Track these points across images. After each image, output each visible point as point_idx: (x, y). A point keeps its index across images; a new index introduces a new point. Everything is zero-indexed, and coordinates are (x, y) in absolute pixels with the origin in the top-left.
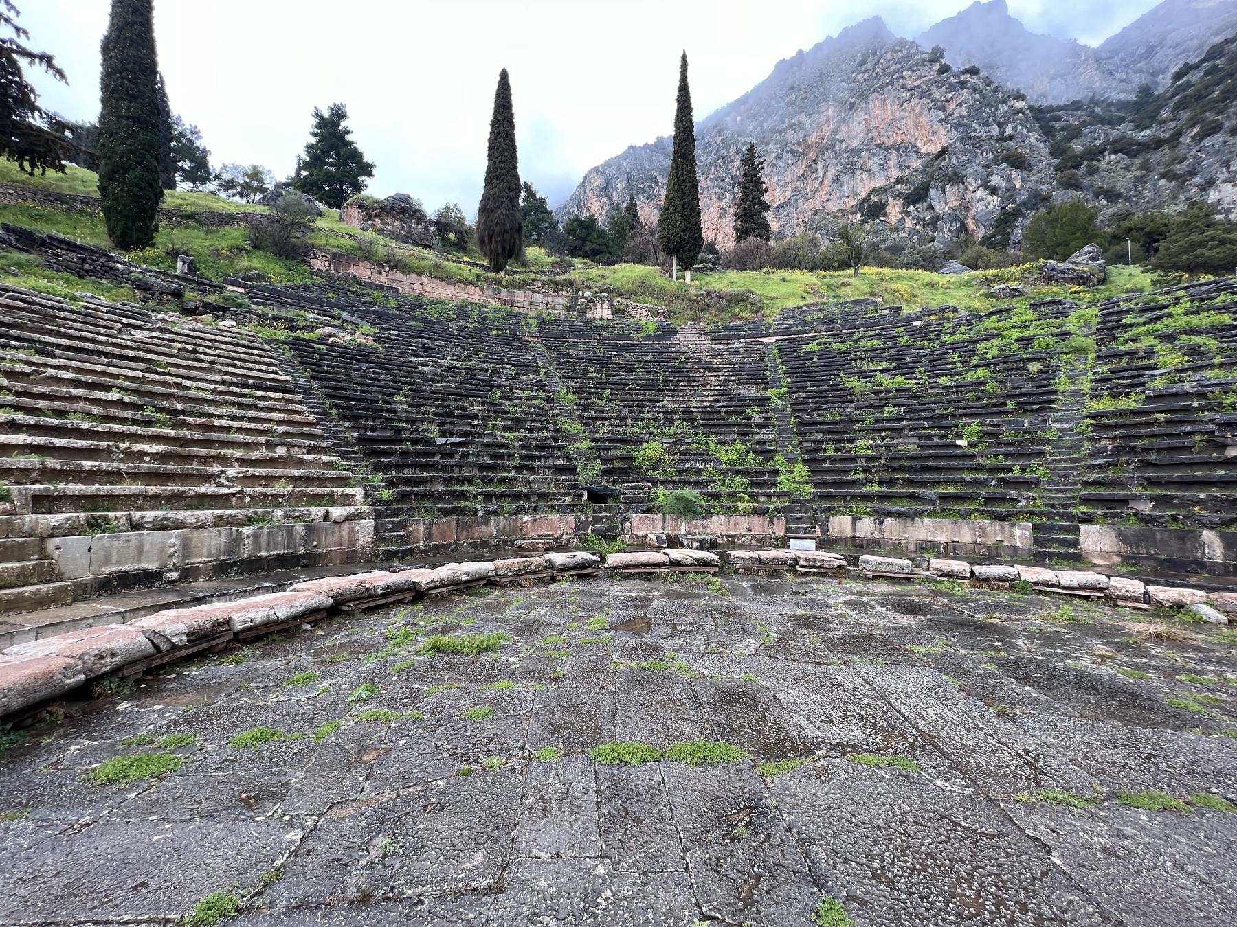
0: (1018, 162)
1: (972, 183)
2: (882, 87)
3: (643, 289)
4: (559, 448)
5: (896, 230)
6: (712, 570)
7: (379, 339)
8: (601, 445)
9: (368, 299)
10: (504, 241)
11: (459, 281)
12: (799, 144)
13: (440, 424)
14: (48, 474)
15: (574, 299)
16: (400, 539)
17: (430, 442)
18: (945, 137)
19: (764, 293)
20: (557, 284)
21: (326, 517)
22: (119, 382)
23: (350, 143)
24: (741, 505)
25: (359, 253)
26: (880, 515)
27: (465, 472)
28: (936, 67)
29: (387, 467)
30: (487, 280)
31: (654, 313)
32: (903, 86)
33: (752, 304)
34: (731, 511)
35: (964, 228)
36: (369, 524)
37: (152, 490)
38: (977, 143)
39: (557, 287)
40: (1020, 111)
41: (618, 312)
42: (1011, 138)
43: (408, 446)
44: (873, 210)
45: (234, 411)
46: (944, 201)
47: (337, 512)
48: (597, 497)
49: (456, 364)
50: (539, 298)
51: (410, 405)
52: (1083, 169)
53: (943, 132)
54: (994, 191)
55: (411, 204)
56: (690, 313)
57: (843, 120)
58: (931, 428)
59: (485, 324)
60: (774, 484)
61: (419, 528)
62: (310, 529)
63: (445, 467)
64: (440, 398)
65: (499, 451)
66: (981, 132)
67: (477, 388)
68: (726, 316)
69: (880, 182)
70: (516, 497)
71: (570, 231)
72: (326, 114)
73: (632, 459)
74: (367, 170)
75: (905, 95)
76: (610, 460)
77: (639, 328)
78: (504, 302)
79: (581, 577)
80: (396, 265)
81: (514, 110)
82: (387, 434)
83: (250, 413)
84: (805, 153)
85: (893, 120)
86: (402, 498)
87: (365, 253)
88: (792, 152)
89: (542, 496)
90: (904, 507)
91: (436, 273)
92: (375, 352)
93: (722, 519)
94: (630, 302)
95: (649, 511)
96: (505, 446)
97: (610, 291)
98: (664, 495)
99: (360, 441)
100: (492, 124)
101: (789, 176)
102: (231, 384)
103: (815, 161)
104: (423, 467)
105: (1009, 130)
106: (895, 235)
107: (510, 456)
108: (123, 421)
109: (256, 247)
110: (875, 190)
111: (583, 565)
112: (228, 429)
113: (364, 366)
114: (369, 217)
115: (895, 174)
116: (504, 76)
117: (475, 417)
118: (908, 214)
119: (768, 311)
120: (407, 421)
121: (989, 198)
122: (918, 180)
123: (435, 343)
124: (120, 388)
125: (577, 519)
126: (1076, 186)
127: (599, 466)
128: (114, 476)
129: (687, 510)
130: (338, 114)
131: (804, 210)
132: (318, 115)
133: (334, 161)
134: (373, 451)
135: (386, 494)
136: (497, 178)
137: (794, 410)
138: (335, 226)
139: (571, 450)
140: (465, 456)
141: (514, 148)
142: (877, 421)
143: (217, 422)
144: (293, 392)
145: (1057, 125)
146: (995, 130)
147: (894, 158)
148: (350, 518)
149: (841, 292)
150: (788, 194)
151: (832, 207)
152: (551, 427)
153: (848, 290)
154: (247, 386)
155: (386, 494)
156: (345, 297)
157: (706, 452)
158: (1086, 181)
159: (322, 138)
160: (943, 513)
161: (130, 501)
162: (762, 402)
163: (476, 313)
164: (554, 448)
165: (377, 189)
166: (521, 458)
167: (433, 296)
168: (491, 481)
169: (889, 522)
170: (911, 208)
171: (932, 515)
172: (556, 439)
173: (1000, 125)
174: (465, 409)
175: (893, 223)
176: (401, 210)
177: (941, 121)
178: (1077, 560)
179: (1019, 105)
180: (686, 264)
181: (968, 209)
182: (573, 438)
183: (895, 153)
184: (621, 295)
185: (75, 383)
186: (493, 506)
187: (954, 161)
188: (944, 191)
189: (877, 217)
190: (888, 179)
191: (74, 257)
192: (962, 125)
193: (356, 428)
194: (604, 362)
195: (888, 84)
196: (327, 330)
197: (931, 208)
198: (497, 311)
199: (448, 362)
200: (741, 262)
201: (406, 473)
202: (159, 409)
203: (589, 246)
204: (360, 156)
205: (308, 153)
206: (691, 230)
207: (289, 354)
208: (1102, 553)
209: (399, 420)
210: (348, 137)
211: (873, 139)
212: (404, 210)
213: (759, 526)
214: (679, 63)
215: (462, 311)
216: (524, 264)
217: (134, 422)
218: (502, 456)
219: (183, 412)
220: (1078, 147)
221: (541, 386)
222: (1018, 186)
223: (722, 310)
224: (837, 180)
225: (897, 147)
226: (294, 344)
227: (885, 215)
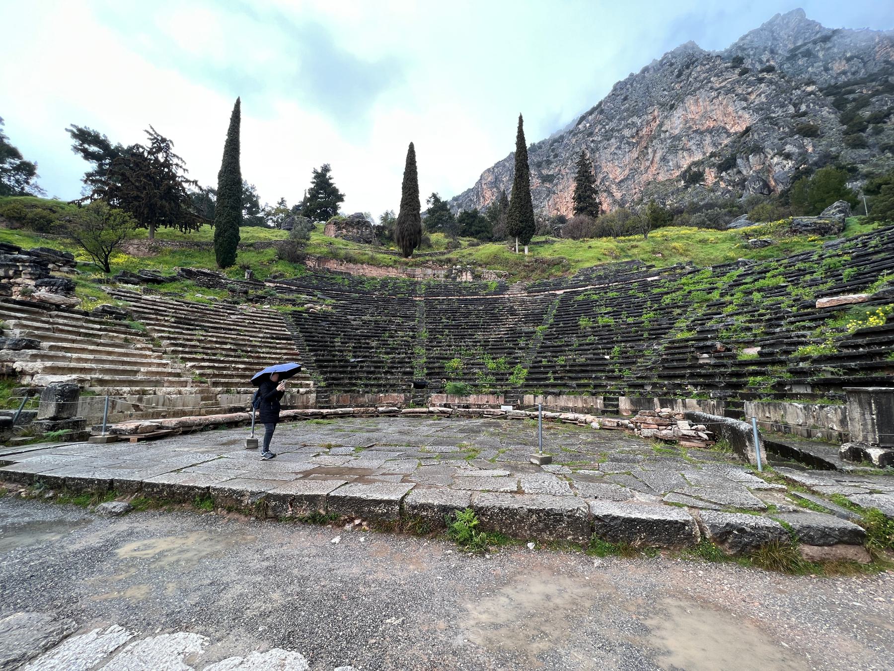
0: (810, 132)
1: (770, 152)
2: (695, 91)
3: (494, 261)
4: (409, 363)
5: (713, 191)
6: (446, 415)
7: (335, 307)
8: (431, 360)
9: (334, 282)
10: (410, 240)
11: (384, 266)
12: (633, 137)
13: (355, 352)
14: (215, 376)
15: (450, 271)
16: (326, 402)
17: (348, 361)
18: (748, 119)
19: (573, 258)
20: (441, 261)
21: (298, 392)
22: (230, 341)
23: (332, 184)
24: (484, 390)
25: (331, 256)
26: (546, 394)
27: (361, 375)
28: (737, 71)
29: (326, 373)
30: (400, 263)
31: (500, 276)
32: (711, 88)
33: (563, 266)
34: (479, 393)
35: (766, 185)
36: (314, 395)
37: (243, 381)
38: (774, 122)
39: (441, 263)
40: (810, 94)
41: (476, 277)
42: (805, 114)
43: (337, 363)
44: (693, 177)
45: (268, 350)
46: (749, 167)
47: (302, 390)
48: (419, 386)
49: (371, 319)
50: (429, 271)
51: (342, 343)
52: (869, 130)
53: (747, 116)
54: (788, 156)
55: (363, 218)
56: (523, 274)
57: (666, 117)
58: (603, 349)
59: (396, 289)
60: (507, 380)
61: (334, 398)
62: (292, 396)
63: (351, 372)
64: (358, 338)
65: (378, 364)
66: (778, 113)
67: (378, 331)
68: (546, 275)
69: (698, 157)
70: (380, 386)
71: (461, 220)
72: (320, 171)
73: (443, 368)
74: (340, 198)
75: (714, 94)
76: (433, 368)
77: (486, 287)
78: (409, 275)
79: (390, 416)
80: (350, 260)
81: (417, 164)
82: (329, 358)
83: (274, 351)
84: (638, 143)
85: (706, 112)
86: (329, 385)
87: (334, 255)
88: (628, 143)
89: (391, 386)
90: (556, 390)
91: (373, 262)
92: (332, 314)
93: (475, 396)
94: (485, 270)
95: (441, 392)
96: (382, 362)
97: (474, 264)
98: (449, 385)
99: (316, 361)
100: (405, 174)
101: (627, 159)
102: (267, 338)
103: (646, 148)
104: (341, 373)
105: (803, 108)
106: (712, 194)
107: (383, 367)
108: (232, 356)
109: (280, 258)
110: (695, 164)
111: (390, 412)
112: (265, 358)
113: (323, 324)
114: (339, 229)
115: (710, 150)
116: (411, 146)
117: (373, 348)
118: (722, 178)
119: (572, 270)
120: (339, 351)
121: (785, 162)
122: (728, 153)
123: (363, 306)
124: (231, 343)
125: (406, 396)
126: (862, 145)
127: (425, 371)
128: (231, 376)
129: (459, 392)
130: (326, 169)
131: (640, 182)
132: (315, 172)
133: (323, 196)
134: (321, 365)
135: (323, 384)
136: (407, 204)
137: (544, 339)
138: (322, 236)
139: (414, 363)
140: (362, 367)
141: (417, 186)
142: (580, 345)
143: (262, 355)
144: (291, 340)
145: (851, 97)
146: (791, 110)
147: (708, 139)
148: (307, 393)
149: (630, 253)
150: (627, 172)
151: (661, 178)
152: (409, 352)
153: (635, 251)
154: (273, 338)
155: (323, 384)
156: (322, 283)
157: (483, 364)
158: (871, 140)
159: (317, 184)
160: (573, 393)
161: (236, 384)
162: (529, 335)
163: (391, 284)
164: (407, 363)
165: (346, 209)
166: (389, 368)
167: (369, 275)
168: (370, 379)
169: (549, 397)
170: (724, 174)
171: (569, 394)
172: (410, 358)
173: (795, 105)
174: (368, 344)
175: (710, 185)
176: (359, 221)
177: (744, 108)
178: (617, 413)
179: (810, 89)
180: (525, 242)
181: (769, 171)
182: (420, 357)
183: (709, 136)
184: (480, 265)
185: (216, 342)
186: (367, 390)
187: (756, 136)
188: (748, 159)
189: (697, 182)
190: (704, 154)
191: (206, 279)
192: (762, 110)
193: (315, 355)
194: (454, 312)
195: (699, 88)
196: (309, 305)
197: (739, 172)
198: (404, 282)
199: (367, 318)
200: (576, 233)
201: (334, 375)
202: (243, 351)
203: (473, 228)
204: (337, 191)
205: (310, 193)
206: (527, 221)
207: (292, 320)
208: (626, 410)
209: (335, 351)
210: (331, 181)
211: (690, 127)
212: (359, 222)
213: (492, 399)
214: (518, 121)
215: (384, 283)
216: (430, 246)
217: (235, 357)
218: (379, 367)
219: (250, 352)
220: (866, 113)
221: (412, 329)
222: (810, 150)
223: (543, 271)
224: (664, 159)
225: (710, 131)
226: (294, 314)
227: (703, 180)
